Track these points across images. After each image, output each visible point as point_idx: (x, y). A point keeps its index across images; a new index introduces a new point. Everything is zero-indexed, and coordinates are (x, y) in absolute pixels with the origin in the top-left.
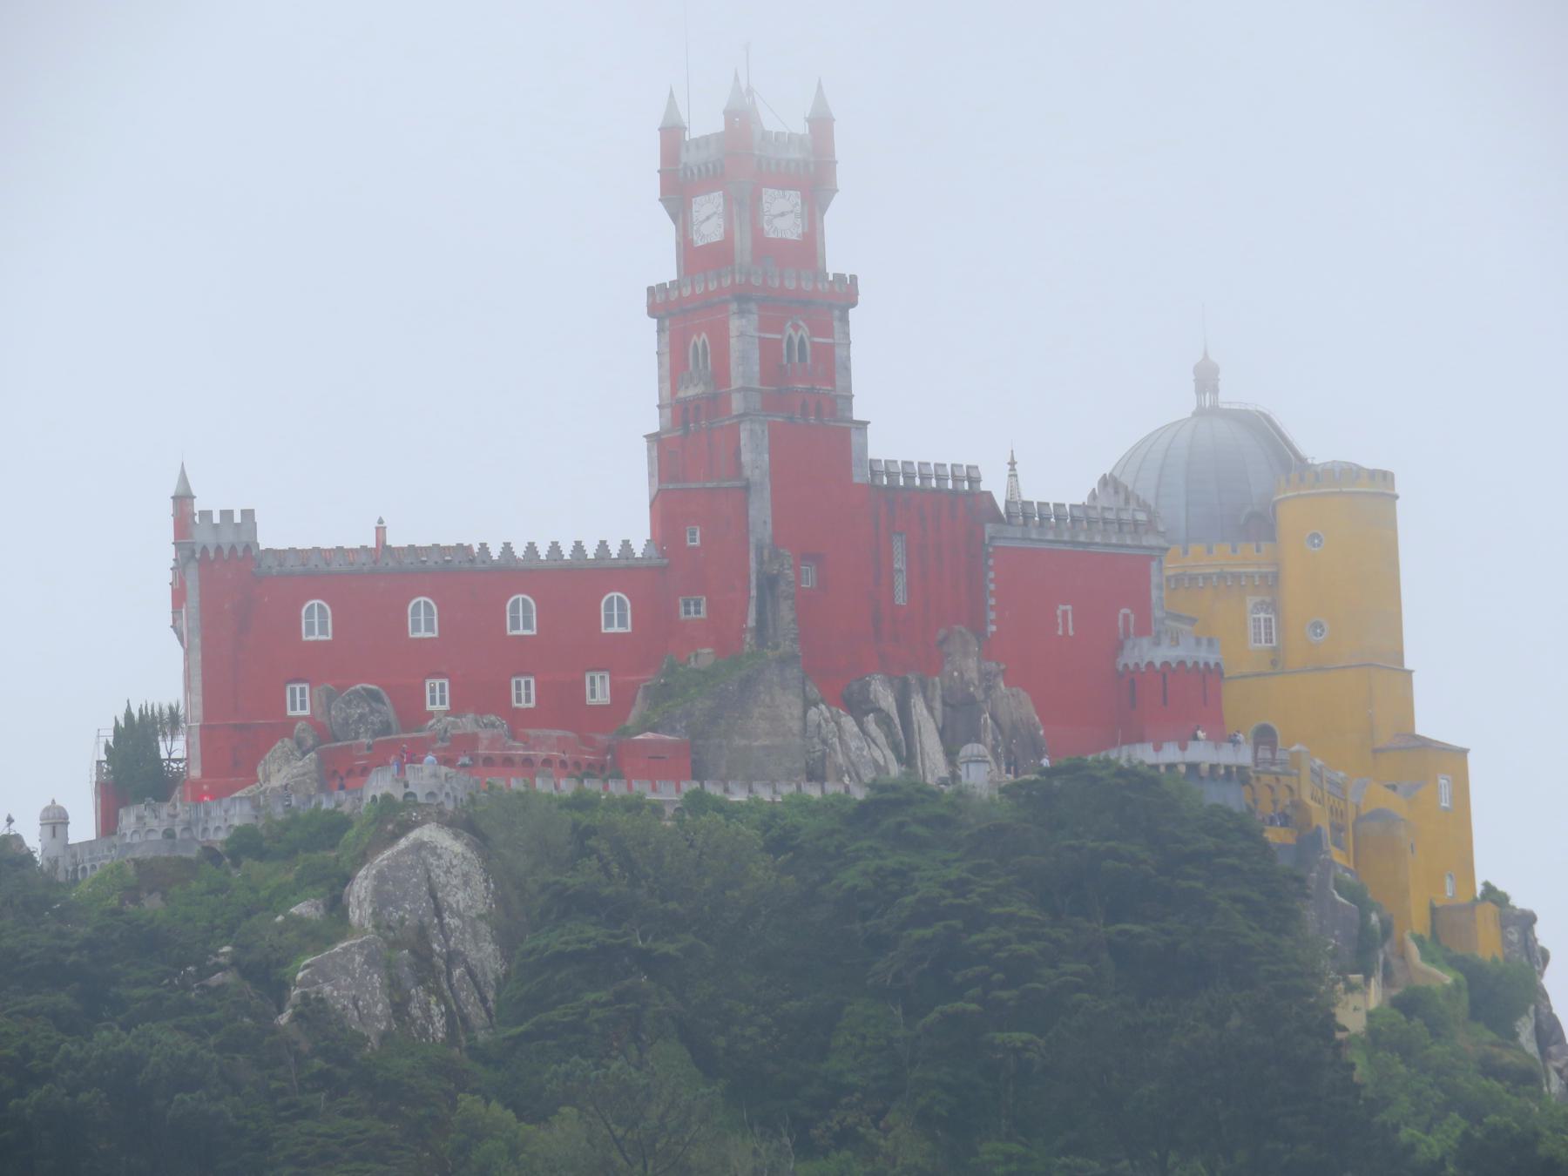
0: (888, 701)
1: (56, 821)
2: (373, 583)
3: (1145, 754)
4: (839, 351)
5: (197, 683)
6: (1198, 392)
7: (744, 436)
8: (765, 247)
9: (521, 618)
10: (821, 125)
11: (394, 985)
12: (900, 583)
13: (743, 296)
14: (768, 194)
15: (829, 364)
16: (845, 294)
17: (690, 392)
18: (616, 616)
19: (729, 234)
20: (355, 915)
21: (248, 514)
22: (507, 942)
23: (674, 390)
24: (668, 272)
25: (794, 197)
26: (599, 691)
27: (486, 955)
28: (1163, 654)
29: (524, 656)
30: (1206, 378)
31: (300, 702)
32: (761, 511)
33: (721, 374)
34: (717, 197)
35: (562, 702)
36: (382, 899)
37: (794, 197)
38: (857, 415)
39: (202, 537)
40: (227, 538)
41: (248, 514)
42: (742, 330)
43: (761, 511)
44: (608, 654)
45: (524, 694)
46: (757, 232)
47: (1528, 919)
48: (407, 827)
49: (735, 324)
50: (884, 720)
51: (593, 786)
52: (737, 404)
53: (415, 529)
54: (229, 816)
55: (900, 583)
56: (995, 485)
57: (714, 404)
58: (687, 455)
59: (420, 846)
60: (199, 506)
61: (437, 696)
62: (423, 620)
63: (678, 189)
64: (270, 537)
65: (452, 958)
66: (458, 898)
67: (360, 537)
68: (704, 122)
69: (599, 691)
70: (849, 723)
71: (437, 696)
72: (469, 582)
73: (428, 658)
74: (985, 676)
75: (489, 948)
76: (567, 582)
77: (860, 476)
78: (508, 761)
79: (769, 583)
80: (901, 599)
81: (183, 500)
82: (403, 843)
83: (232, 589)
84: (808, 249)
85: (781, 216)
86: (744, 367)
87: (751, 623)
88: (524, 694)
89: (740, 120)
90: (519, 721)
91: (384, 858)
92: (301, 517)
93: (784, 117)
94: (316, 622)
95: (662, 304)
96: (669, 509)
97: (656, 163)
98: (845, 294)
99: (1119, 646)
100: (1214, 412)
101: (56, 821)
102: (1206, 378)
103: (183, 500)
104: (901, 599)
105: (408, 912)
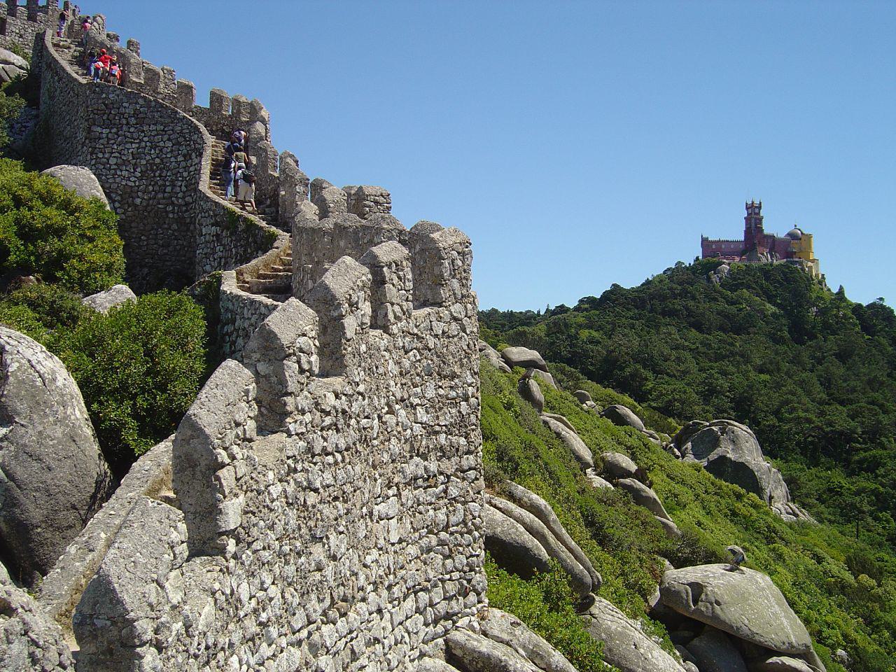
0: (765, 254)
1: (690, 264)
8: (755, 214)
10: (760, 203)
17: (748, 226)
30: (795, 226)
56: (775, 235)
58: (748, 232)
63: (747, 209)
83: (705, 242)
85: (757, 211)
89: (753, 203)
93: (756, 202)
95: (745, 218)
101: (690, 264)
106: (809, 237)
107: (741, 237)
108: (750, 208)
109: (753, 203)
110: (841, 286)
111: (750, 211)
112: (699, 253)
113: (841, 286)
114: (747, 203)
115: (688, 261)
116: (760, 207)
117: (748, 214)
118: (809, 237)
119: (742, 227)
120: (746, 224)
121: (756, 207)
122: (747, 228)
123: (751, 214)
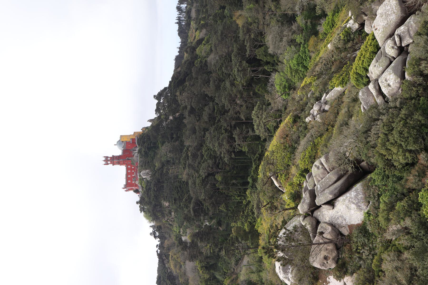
2: (127, 179)
16: (113, 156)
18: (129, 167)
22: (147, 169)
24: (112, 165)
26: (133, 168)
27: (147, 171)
31: (133, 182)
35: (134, 169)
45: (133, 171)
53: (125, 176)
54: (140, 185)
57: (118, 162)
61: (133, 175)
62: (129, 176)
63: (108, 164)
64: (125, 184)
67: (125, 179)
68: (104, 163)
69: (133, 168)
71: (133, 175)
73: (131, 176)
76: (127, 169)
81: (123, 188)
84: (111, 158)
88: (133, 171)
89: (104, 161)
93: (104, 159)
94: (129, 181)
95: (113, 165)
98: (113, 156)
103: (123, 188)
106: (121, 136)
108: (107, 162)
109: (104, 161)
111: (109, 162)
112: (132, 192)
114: (105, 164)
115: (137, 197)
116: (107, 157)
117: (111, 164)
118: (121, 136)
119: (118, 167)
120: (116, 164)
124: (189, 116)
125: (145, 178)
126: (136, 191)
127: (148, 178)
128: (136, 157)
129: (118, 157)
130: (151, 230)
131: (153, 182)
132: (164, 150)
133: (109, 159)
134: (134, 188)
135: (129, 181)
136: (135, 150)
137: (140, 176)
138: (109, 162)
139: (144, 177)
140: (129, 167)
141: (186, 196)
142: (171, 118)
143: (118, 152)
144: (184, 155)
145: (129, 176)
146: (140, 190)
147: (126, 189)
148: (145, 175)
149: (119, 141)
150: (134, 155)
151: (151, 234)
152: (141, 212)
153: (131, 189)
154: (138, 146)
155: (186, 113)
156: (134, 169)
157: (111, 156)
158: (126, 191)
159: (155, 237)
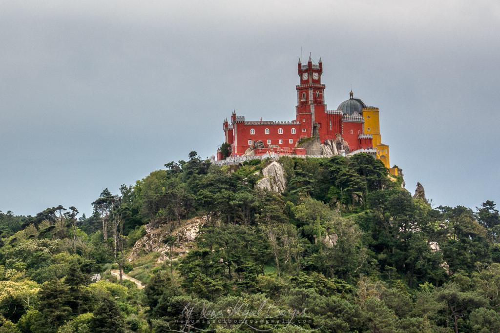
0: (330, 143)
2: (260, 127)
3: (363, 151)
4: (323, 95)
5: (228, 139)
6: (350, 96)
7: (311, 107)
8: (314, 81)
9: (281, 131)
10: (320, 64)
11: (271, 185)
12: (331, 127)
13: (311, 87)
14: (314, 73)
15: (321, 96)
17: (303, 100)
18: (294, 131)
19: (308, 79)
20: (264, 174)
21: (243, 117)
23: (300, 100)
24: (299, 84)
25: (317, 73)
26: (291, 141)
28: (364, 137)
29: (281, 137)
30: (351, 94)
31: (250, 143)
32: (313, 117)
33: (307, 98)
34: (307, 74)
36: (269, 172)
37: (317, 73)
38: (325, 104)
39: (237, 120)
40: (240, 120)
41: (243, 117)
42: (311, 92)
43: (313, 117)
44: (292, 136)
45: (281, 142)
46: (312, 79)
47: (402, 170)
48: (271, 162)
49: (310, 91)
50: (330, 146)
51: (294, 156)
52: (310, 103)
55: (331, 127)
57: (306, 102)
59: (274, 165)
60: (236, 116)
61: (269, 142)
62: (267, 132)
63: (301, 72)
64: (246, 120)
65: (279, 180)
66: (279, 172)
68: (305, 63)
70: (326, 146)
71: (269, 142)
72: (274, 127)
73: (268, 137)
74: (342, 140)
75: (283, 179)
76: (287, 127)
77: (326, 112)
78: (281, 152)
79: (315, 127)
80: (331, 129)
81: (234, 116)
82: (271, 164)
84: (318, 81)
86: (311, 98)
87: (312, 132)
88: (281, 142)
89: (310, 63)
90: (280, 146)
91: (269, 166)
92: (250, 118)
93: (315, 63)
94: (253, 132)
95: (298, 88)
96: (300, 117)
97: (297, 68)
98: (323, 88)
99: (359, 135)
100: (353, 99)
102: (351, 94)
103: (234, 116)
104: (331, 129)
105: (272, 174)
106: (375, 111)
107: (291, 117)
108: (305, 71)
109: (310, 63)
110: (419, 184)
113: (419, 184)
114: (300, 65)
117: (302, 82)
118: (375, 111)
119: (294, 100)
120: (300, 96)
121: (316, 71)
122: (302, 103)
123: (307, 81)
124: (443, 298)
125: (261, 173)
126: (225, 152)
127: (263, 184)
128: (322, 151)
129: (319, 102)
130: (117, 193)
131: (250, 196)
132: (338, 227)
133: (315, 76)
134: (235, 143)
135: (253, 132)
136: (339, 148)
137: (268, 161)
138: (305, 76)
139: (265, 171)
140: (294, 131)
141: (217, 283)
142: (434, 246)
143: (333, 103)
144: (331, 282)
145: (267, 132)
146: (230, 160)
147: (230, 122)
148: (272, 177)
149: (363, 106)
150: (326, 144)
151: (106, 193)
152: (167, 165)
153: (231, 138)
154: (352, 154)
155: (450, 289)
156: (286, 143)
157: (322, 83)
158: (226, 124)
159: (99, 203)
